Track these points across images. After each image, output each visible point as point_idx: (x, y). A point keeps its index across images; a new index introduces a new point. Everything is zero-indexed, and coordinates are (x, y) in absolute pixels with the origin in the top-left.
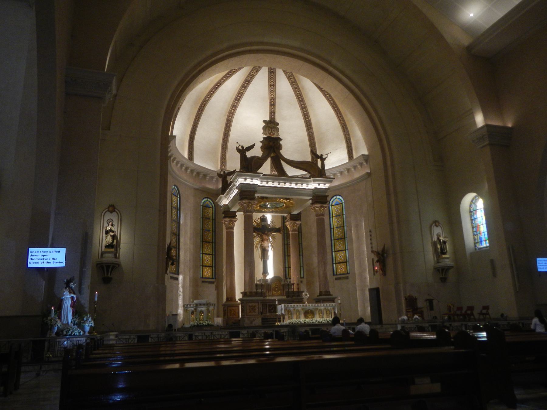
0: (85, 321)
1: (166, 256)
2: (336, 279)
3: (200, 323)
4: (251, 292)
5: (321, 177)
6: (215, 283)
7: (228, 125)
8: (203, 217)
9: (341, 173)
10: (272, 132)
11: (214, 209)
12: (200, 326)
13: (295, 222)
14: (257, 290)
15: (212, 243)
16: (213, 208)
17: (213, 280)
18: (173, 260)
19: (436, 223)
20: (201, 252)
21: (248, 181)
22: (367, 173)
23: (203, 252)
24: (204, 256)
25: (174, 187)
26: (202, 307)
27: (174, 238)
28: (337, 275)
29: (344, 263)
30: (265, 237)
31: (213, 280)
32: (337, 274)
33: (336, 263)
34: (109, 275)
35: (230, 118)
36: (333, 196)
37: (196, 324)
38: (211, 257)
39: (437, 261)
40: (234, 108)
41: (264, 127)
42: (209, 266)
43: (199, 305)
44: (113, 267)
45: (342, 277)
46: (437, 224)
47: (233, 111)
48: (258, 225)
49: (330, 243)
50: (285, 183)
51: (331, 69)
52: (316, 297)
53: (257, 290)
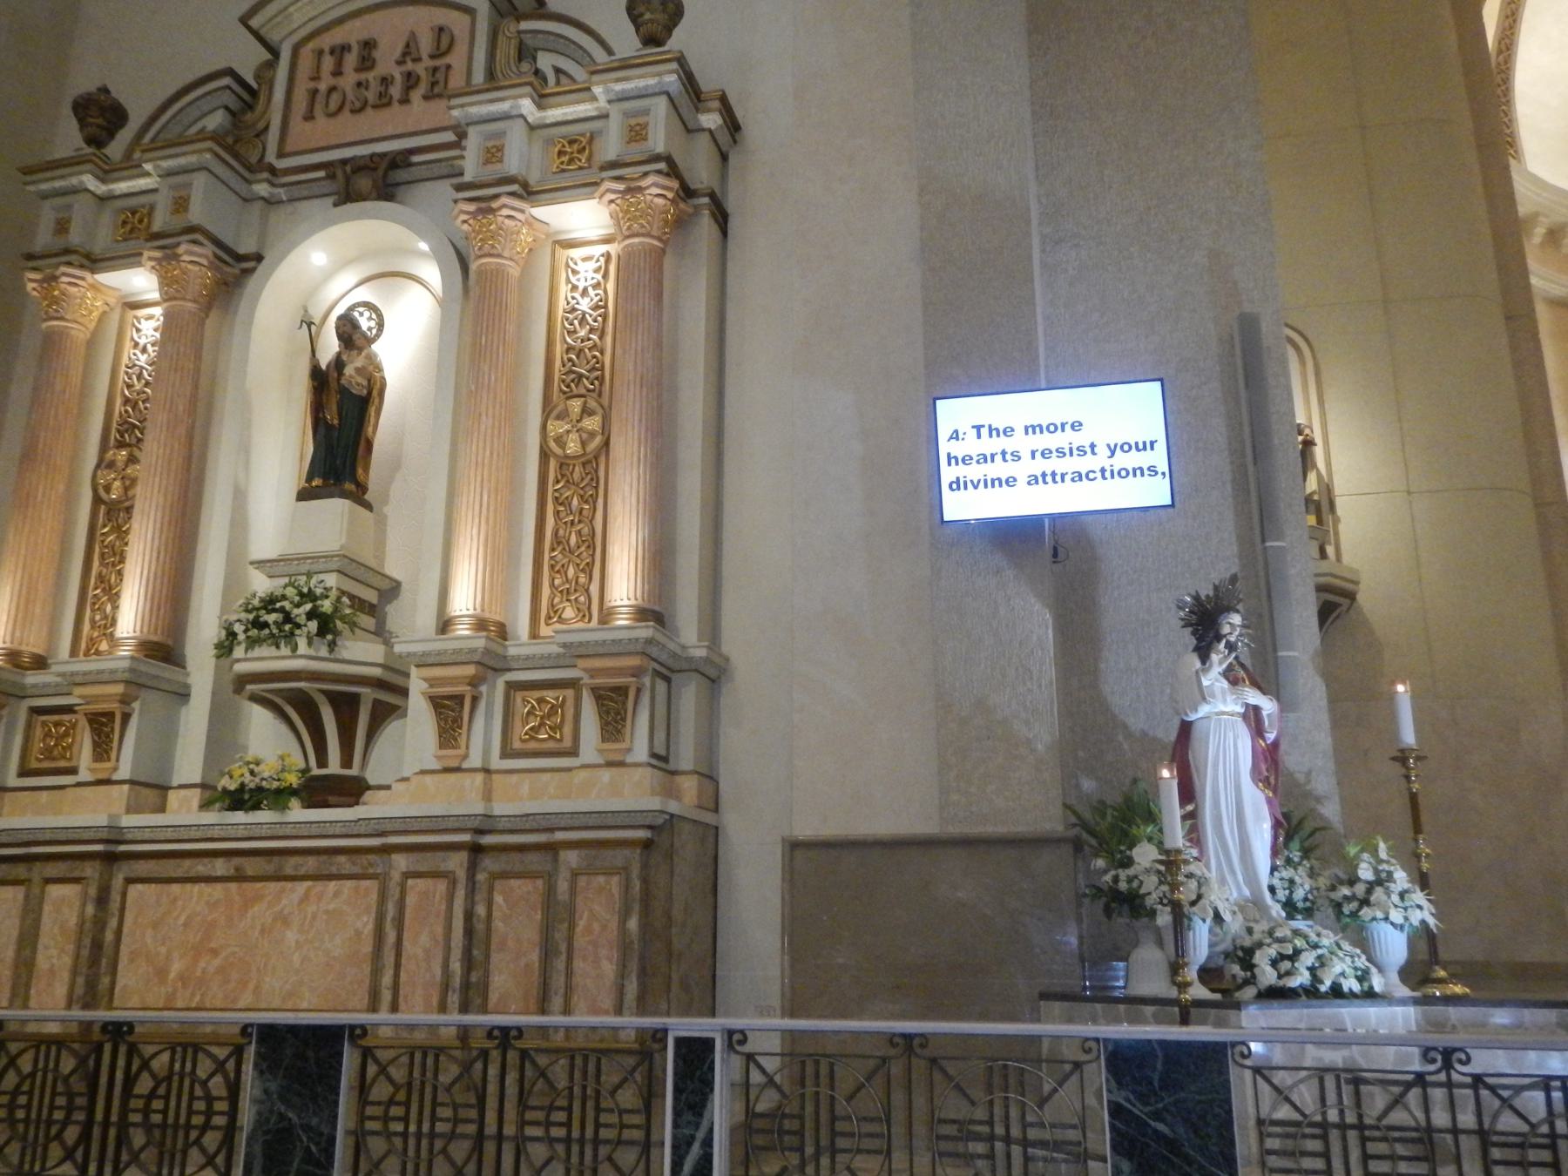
0: (1369, 891)
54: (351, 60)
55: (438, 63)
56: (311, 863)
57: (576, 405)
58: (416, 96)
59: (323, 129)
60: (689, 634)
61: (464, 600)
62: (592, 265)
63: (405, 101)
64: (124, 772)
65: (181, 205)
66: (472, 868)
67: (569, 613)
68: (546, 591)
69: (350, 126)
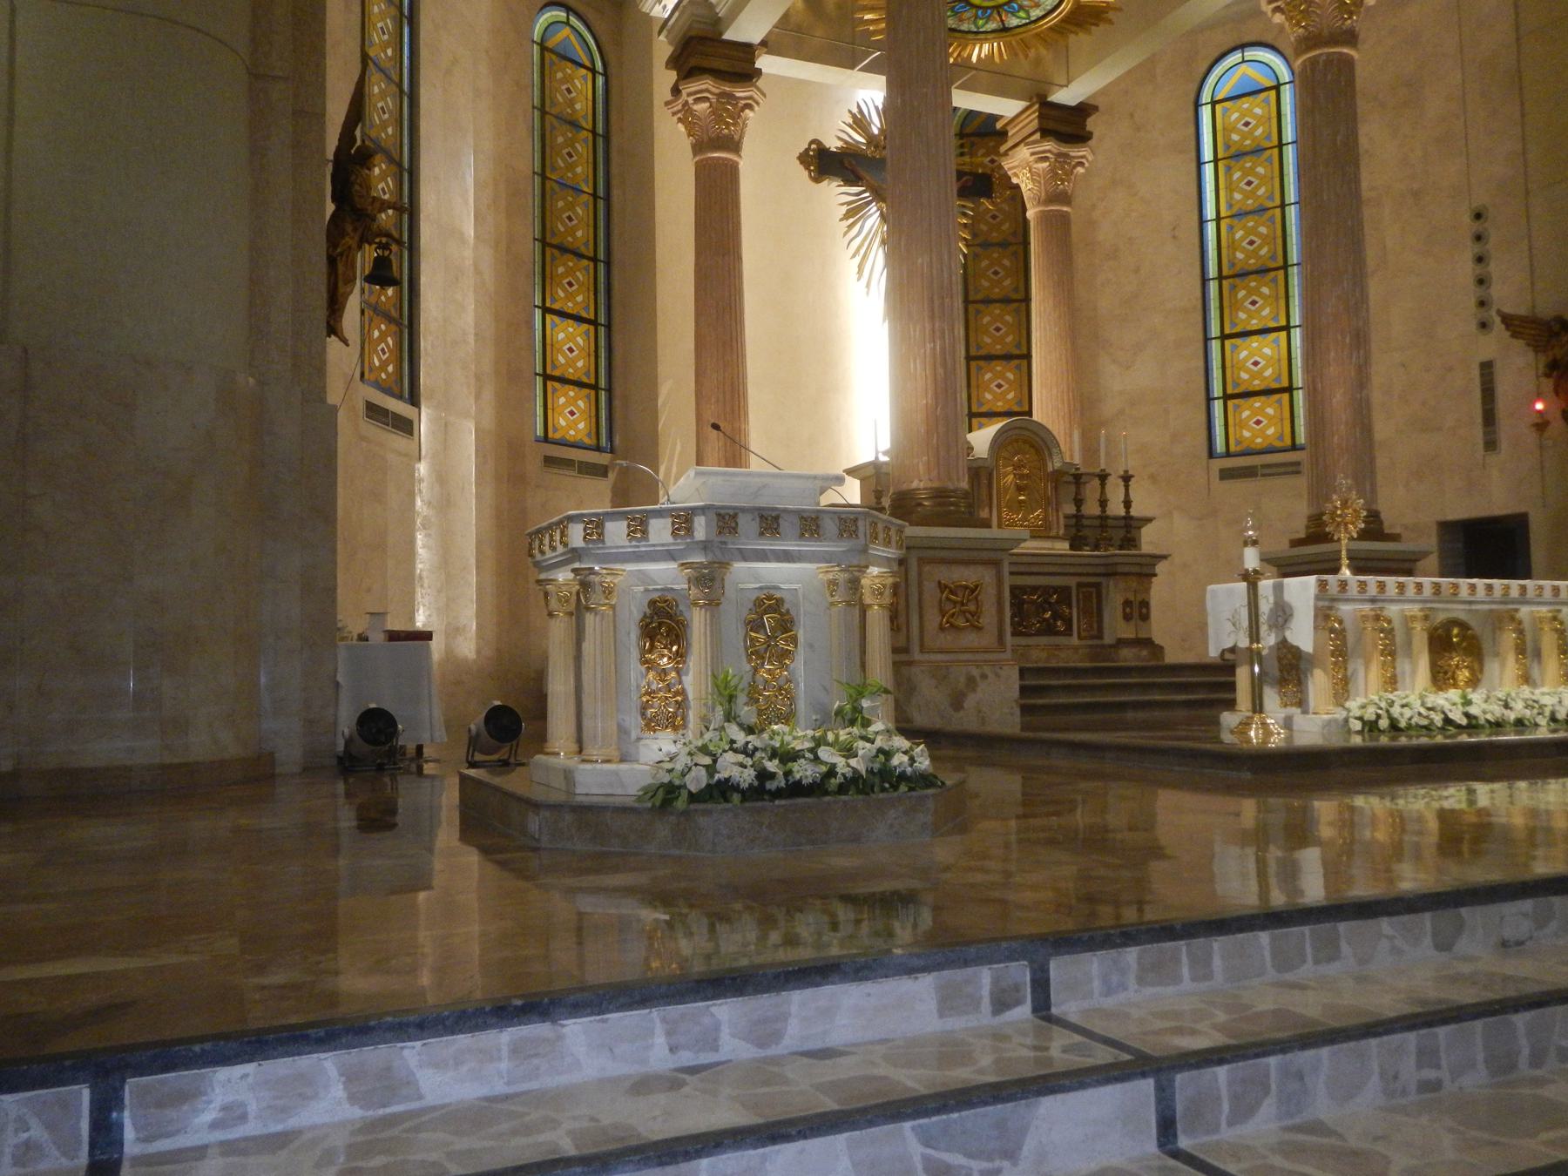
1: (330, 208)
2: (1226, 474)
3: (788, 756)
4: (940, 495)
6: (612, 476)
11: (600, 80)
12: (796, 789)
13: (1064, 149)
15: (595, 260)
16: (593, 71)
17: (603, 459)
18: (387, 240)
20: (538, 302)
23: (548, 305)
24: (554, 325)
26: (787, 557)
27: (382, 339)
28: (1228, 454)
29: (1277, 397)
31: (603, 459)
32: (1233, 448)
33: (1226, 397)
36: (1225, 48)
37: (733, 768)
38: (587, 333)
42: (579, 384)
43: (747, 524)
45: (1263, 466)
48: (876, 147)
49: (1198, 293)
52: (1281, 547)
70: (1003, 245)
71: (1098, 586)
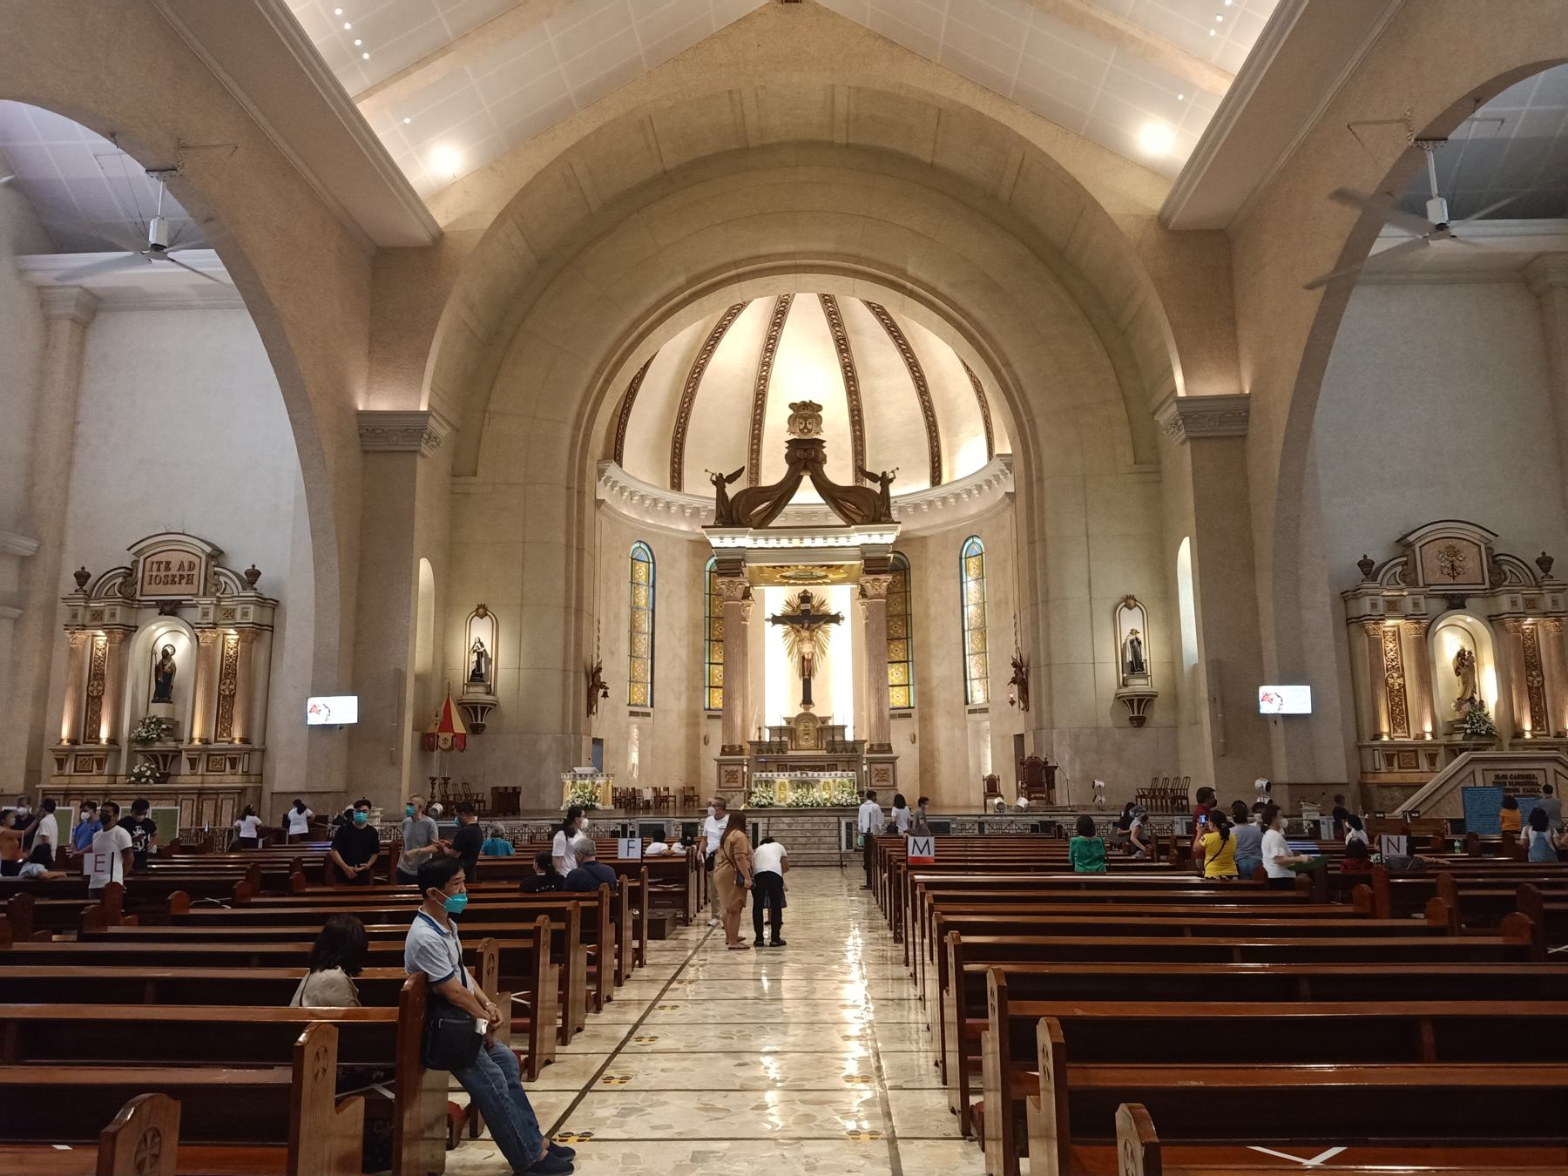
2: (970, 712)
5: (879, 522)
7: (760, 402)
8: (710, 594)
9: (969, 492)
10: (806, 427)
14: (781, 738)
19: (1129, 602)
20: (707, 661)
21: (728, 542)
22: (1007, 493)
24: (713, 668)
25: (638, 545)
30: (805, 634)
34: (479, 722)
35: (762, 388)
39: (1123, 682)
40: (765, 368)
41: (791, 416)
44: (483, 709)
46: (1132, 602)
47: (764, 373)
50: (801, 539)
51: (909, 285)
53: (781, 738)
54: (163, 566)
55: (190, 573)
56: (158, 796)
57: (228, 681)
58: (184, 581)
59: (153, 588)
60: (256, 743)
61: (197, 733)
62: (233, 641)
63: (180, 583)
64: (106, 773)
65: (113, 615)
66: (198, 798)
67: (225, 735)
68: (219, 729)
69: (162, 589)
70: (898, 616)
71: (836, 765)
